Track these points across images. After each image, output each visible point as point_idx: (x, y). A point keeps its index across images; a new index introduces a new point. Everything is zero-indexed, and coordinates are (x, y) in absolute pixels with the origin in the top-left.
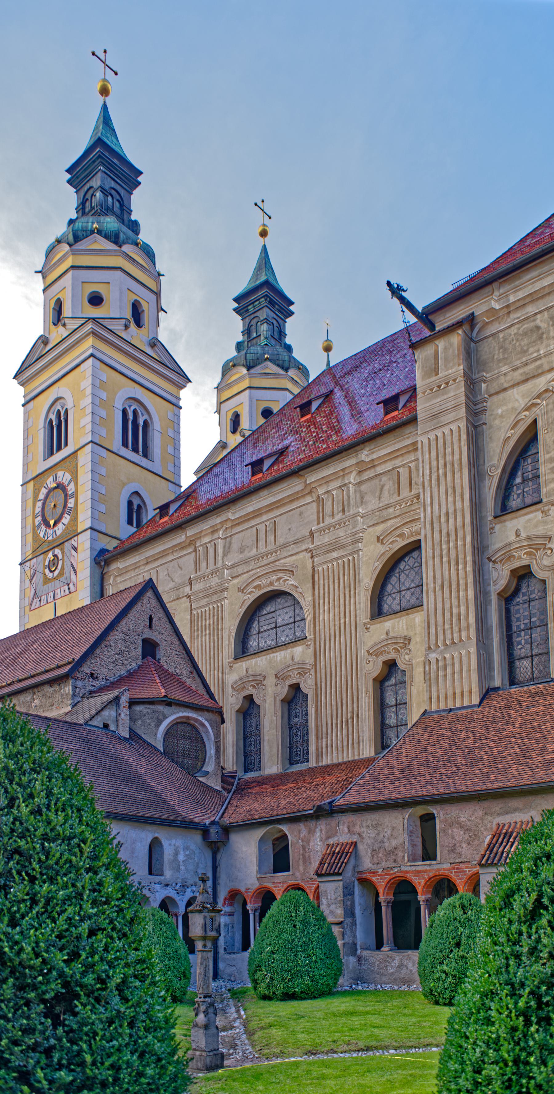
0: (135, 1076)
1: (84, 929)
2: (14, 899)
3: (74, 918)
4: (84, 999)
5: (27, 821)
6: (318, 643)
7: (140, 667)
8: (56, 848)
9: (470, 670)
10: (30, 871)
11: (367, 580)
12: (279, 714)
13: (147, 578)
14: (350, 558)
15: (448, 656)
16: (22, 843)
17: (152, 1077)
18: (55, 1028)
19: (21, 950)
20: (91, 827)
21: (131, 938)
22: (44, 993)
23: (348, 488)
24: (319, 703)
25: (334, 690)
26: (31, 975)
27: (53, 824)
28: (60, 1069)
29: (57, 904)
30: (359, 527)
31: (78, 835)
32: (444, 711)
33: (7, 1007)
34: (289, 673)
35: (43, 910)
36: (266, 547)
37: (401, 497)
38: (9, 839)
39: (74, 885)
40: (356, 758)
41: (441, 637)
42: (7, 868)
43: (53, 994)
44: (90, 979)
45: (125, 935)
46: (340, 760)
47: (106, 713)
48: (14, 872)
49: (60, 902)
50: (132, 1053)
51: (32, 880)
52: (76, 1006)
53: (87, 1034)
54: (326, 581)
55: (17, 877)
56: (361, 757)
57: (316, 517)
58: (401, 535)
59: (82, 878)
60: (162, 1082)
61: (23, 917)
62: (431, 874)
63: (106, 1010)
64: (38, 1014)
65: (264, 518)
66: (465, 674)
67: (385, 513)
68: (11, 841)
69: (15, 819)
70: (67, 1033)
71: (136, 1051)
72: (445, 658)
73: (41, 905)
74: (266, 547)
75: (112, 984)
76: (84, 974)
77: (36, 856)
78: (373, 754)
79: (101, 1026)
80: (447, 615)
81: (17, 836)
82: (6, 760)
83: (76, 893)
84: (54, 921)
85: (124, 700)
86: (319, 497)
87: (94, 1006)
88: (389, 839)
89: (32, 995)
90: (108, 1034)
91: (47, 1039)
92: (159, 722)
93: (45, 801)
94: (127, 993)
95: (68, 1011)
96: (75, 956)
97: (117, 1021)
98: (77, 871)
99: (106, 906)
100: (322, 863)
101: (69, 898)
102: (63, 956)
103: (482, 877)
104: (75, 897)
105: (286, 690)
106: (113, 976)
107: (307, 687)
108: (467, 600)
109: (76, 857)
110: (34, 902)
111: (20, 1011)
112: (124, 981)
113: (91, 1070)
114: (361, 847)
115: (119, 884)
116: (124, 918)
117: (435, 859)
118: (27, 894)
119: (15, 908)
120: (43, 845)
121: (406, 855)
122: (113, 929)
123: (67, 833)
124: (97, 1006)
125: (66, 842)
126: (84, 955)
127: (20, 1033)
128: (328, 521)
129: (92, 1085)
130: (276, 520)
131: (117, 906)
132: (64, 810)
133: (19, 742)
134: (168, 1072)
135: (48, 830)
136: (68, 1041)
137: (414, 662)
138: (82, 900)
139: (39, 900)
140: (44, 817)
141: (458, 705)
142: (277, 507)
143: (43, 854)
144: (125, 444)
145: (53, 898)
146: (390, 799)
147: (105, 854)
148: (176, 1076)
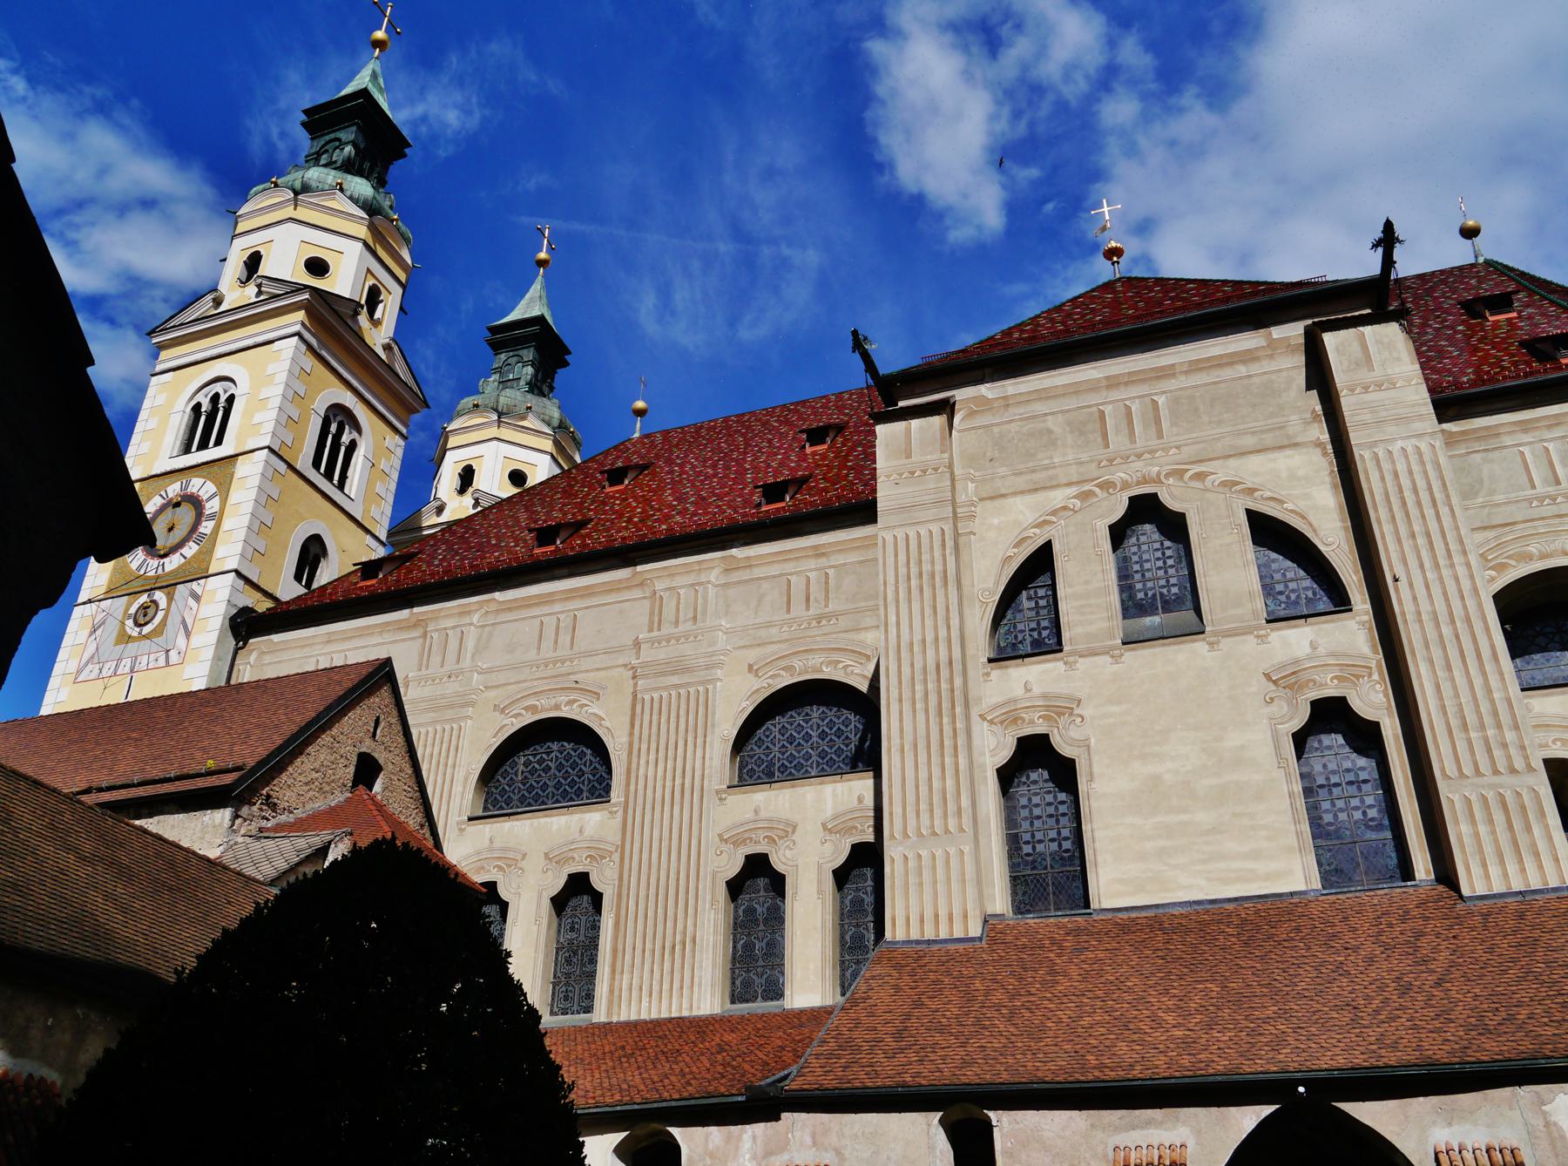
6: (630, 812)
9: (964, 881)
11: (728, 728)
12: (545, 922)
13: (384, 656)
14: (701, 689)
15: (924, 853)
32: (918, 942)
41: (912, 822)
54: (655, 717)
65: (557, 607)
66: (955, 886)
67: (763, 633)
72: (920, 856)
80: (923, 790)
105: (559, 883)
108: (957, 771)
128: (667, 629)
130: (579, 614)
141: (943, 935)
142: (582, 596)
144: (316, 464)
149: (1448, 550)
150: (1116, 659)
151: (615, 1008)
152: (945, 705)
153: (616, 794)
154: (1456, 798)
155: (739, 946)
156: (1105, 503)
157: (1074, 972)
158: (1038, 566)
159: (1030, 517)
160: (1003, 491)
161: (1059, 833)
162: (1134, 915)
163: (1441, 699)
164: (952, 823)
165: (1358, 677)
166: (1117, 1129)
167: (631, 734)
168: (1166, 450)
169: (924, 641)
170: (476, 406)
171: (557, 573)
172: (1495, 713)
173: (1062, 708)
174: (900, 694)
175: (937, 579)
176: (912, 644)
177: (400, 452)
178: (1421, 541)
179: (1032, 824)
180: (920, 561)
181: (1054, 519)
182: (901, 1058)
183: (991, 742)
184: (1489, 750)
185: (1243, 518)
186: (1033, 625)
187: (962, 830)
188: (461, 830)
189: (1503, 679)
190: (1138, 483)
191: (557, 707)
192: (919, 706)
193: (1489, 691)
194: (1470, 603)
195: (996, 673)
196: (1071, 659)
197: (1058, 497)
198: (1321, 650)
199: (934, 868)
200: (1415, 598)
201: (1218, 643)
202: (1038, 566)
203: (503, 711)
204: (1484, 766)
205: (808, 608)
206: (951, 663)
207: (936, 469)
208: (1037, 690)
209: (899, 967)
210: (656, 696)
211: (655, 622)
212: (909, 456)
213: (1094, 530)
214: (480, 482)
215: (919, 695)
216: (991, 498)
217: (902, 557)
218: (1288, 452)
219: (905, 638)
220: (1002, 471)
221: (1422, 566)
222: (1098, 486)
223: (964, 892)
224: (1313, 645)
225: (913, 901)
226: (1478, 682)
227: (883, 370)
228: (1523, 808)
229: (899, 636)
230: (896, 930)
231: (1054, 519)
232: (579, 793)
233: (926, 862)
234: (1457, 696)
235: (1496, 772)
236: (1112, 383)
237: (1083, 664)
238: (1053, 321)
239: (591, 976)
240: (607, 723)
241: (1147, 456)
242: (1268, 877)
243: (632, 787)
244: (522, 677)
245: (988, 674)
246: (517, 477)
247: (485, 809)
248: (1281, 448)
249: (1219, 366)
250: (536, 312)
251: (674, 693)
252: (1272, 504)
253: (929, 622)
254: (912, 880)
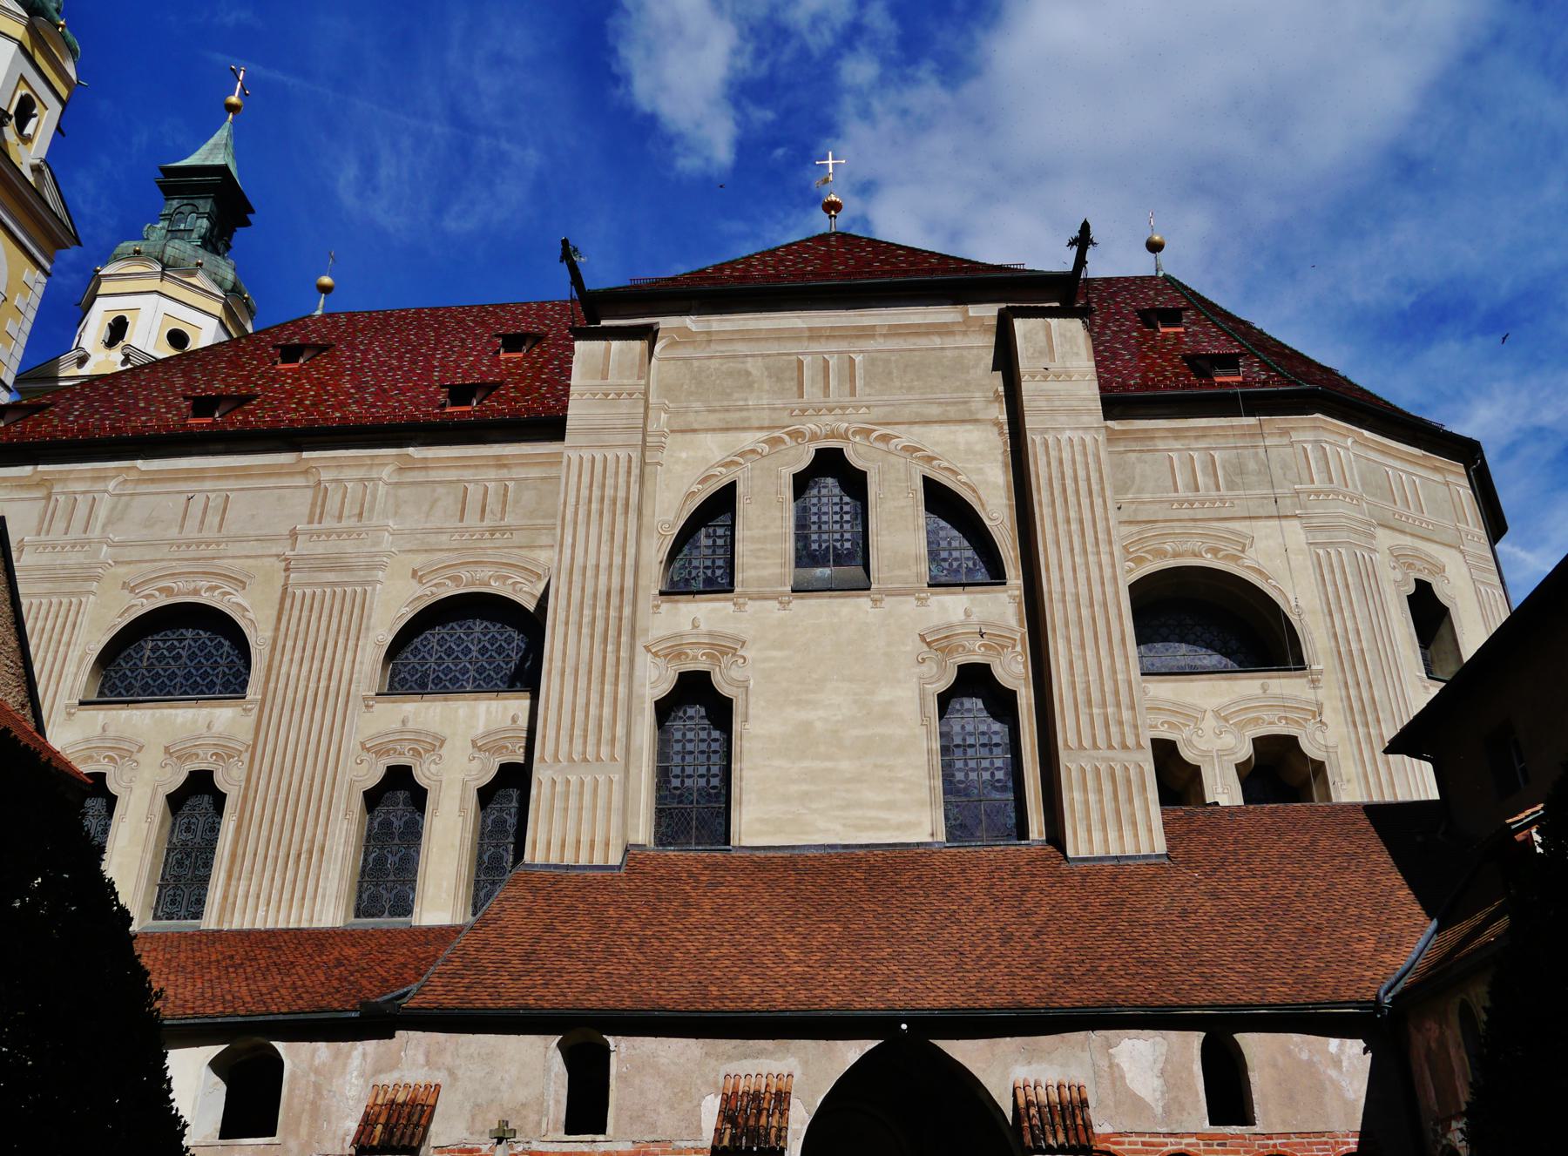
9: (609, 809)
11: (383, 631)
14: (359, 589)
15: (573, 779)
23: (376, 486)
24: (247, 815)
25: (282, 796)
30: (385, 546)
32: (556, 866)
34: (194, 750)
36: (201, 530)
37: (464, 524)
41: (564, 747)
54: (305, 613)
57: (307, 512)
58: (456, 579)
65: (208, 485)
66: (600, 813)
67: (432, 539)
74: (201, 530)
80: (580, 715)
86: (319, 483)
108: (616, 699)
117: (603, 1132)
128: (329, 523)
130: (232, 495)
137: (445, 779)
141: (583, 861)
149: (1096, 539)
150: (784, 605)
151: (228, 916)
152: (612, 632)
153: (253, 692)
154: (1073, 767)
155: (370, 860)
156: (793, 452)
157: (707, 907)
158: (719, 507)
159: (718, 455)
160: (695, 426)
161: (709, 770)
162: (770, 854)
163: (1073, 675)
164: (605, 751)
165: (1003, 647)
166: (730, 1058)
167: (277, 629)
168: (857, 408)
169: (598, 566)
170: (138, 252)
171: (211, 447)
172: (1116, 693)
173: (725, 647)
174: (567, 617)
175: (619, 505)
176: (585, 568)
177: (40, 290)
178: (1074, 527)
179: (683, 759)
180: (603, 485)
181: (741, 460)
182: (526, 981)
183: (654, 674)
184: (1107, 726)
185: (919, 484)
186: (708, 563)
187: (613, 758)
188: (70, 714)
189: (1127, 663)
190: (827, 437)
191: (196, 592)
192: (585, 630)
193: (1114, 672)
194: (1109, 589)
195: (666, 607)
196: (741, 601)
197: (748, 439)
198: (974, 619)
199: (581, 794)
200: (1062, 580)
201: (881, 600)
202: (719, 507)
203: (132, 590)
204: (1101, 742)
205: (482, 519)
206: (622, 591)
207: (630, 395)
208: (704, 628)
209: (534, 890)
210: (308, 591)
211: (317, 512)
212: (605, 377)
213: (779, 477)
214: (133, 337)
215: (586, 620)
216: (682, 431)
217: (585, 479)
218: (969, 427)
219: (579, 561)
220: (697, 405)
221: (1072, 550)
222: (788, 434)
223: (609, 820)
224: (967, 613)
225: (557, 825)
226: (1106, 663)
227: (590, 285)
228: (1129, 781)
229: (573, 559)
230: (536, 853)
231: (741, 460)
232: (211, 686)
233: (574, 788)
234: (1086, 674)
235: (1110, 747)
236: (815, 334)
237: (752, 606)
238: (765, 263)
239: (206, 879)
240: (250, 615)
241: (838, 411)
242: (899, 827)
243: (272, 685)
244: (159, 556)
245: (658, 607)
246: (177, 338)
247: (101, 693)
248: (963, 421)
249: (917, 334)
250: (219, 160)
251: (328, 590)
252: (947, 473)
253: (605, 548)
254: (558, 804)
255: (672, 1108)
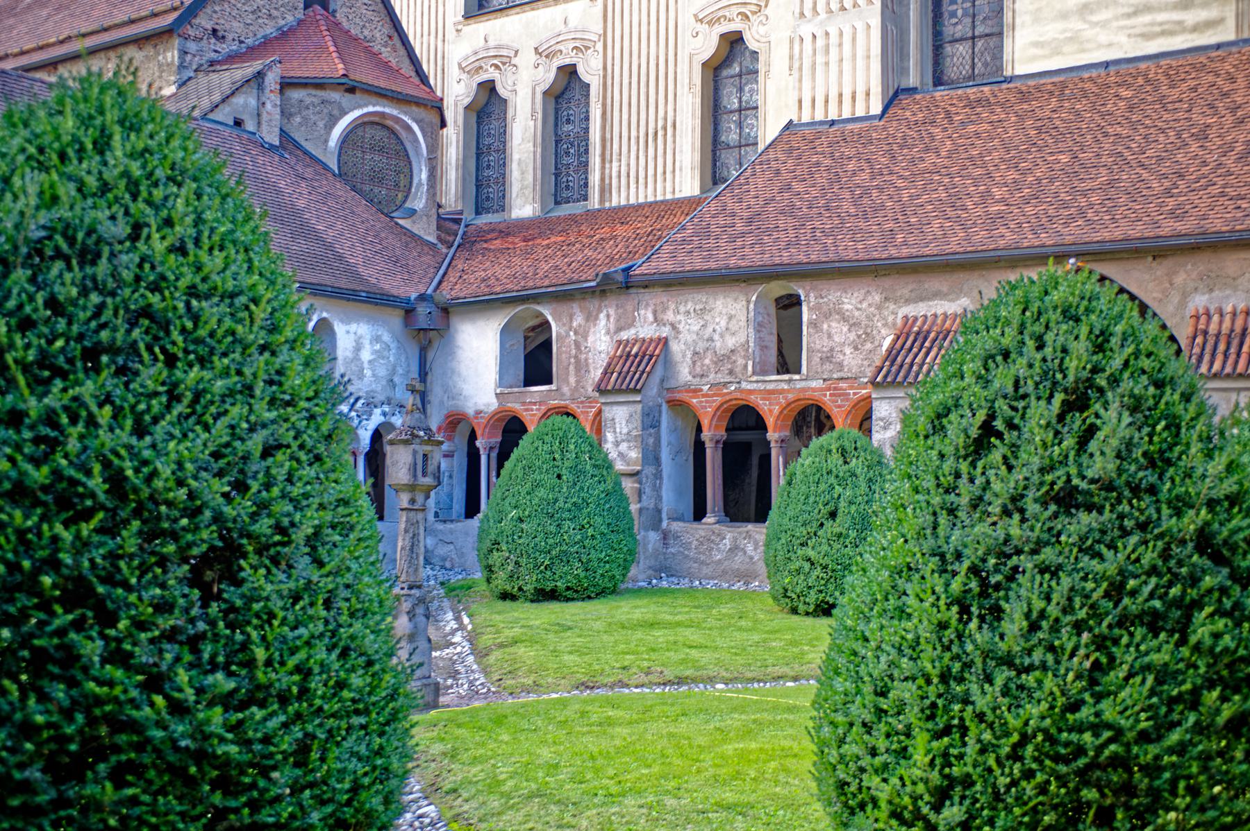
0: (333, 687)
1: (256, 444)
2: (141, 390)
3: (238, 425)
4: (254, 558)
5: (162, 263)
7: (300, 22)
8: (211, 310)
10: (169, 347)
16: (154, 299)
17: (360, 690)
18: (205, 605)
19: (154, 474)
20: (267, 279)
21: (329, 463)
22: (190, 545)
26: (168, 517)
27: (206, 270)
28: (212, 671)
29: (212, 402)
31: (246, 290)
33: (129, 568)
34: (559, 47)
35: (189, 410)
38: (133, 292)
39: (239, 373)
40: (669, 196)
42: (130, 340)
43: (204, 547)
44: (263, 526)
45: (318, 458)
46: (641, 200)
47: (239, 100)
48: (142, 346)
49: (217, 398)
50: (330, 650)
51: (171, 361)
52: (241, 569)
53: (258, 616)
55: (146, 355)
56: (678, 195)
59: (252, 362)
60: (373, 699)
61: (156, 420)
62: (791, 396)
63: (289, 577)
64: (180, 581)
68: (136, 295)
69: (143, 260)
70: (226, 613)
71: (334, 646)
73: (186, 401)
75: (299, 536)
76: (254, 517)
77: (178, 322)
78: (697, 192)
79: (280, 603)
81: (146, 288)
82: (126, 161)
83: (243, 386)
84: (207, 428)
85: (272, 79)
87: (269, 572)
88: (722, 336)
89: (171, 548)
90: (291, 618)
91: (192, 621)
92: (333, 121)
93: (192, 232)
94: (322, 552)
95: (227, 579)
96: (241, 486)
97: (306, 597)
98: (244, 349)
99: (290, 409)
100: (607, 372)
101: (231, 393)
102: (222, 485)
103: (875, 404)
104: (241, 392)
105: (552, 75)
106: (301, 523)
107: (590, 71)
109: (244, 326)
110: (174, 397)
111: (150, 575)
112: (317, 533)
113: (265, 673)
114: (675, 347)
115: (309, 375)
116: (317, 429)
117: (799, 372)
118: (163, 384)
119: (142, 407)
120: (188, 305)
121: (750, 363)
122: (301, 447)
123: (230, 285)
124: (274, 570)
125: (227, 301)
126: (255, 486)
127: (150, 610)
129: (265, 700)
131: (307, 410)
132: (222, 249)
133: (147, 132)
134: (384, 684)
135: (198, 280)
136: (227, 627)
138: (252, 396)
139: (183, 394)
140: (191, 258)
143: (189, 319)
145: (204, 391)
146: (727, 268)
147: (289, 323)
148: (396, 691)
255: (856, 348)
